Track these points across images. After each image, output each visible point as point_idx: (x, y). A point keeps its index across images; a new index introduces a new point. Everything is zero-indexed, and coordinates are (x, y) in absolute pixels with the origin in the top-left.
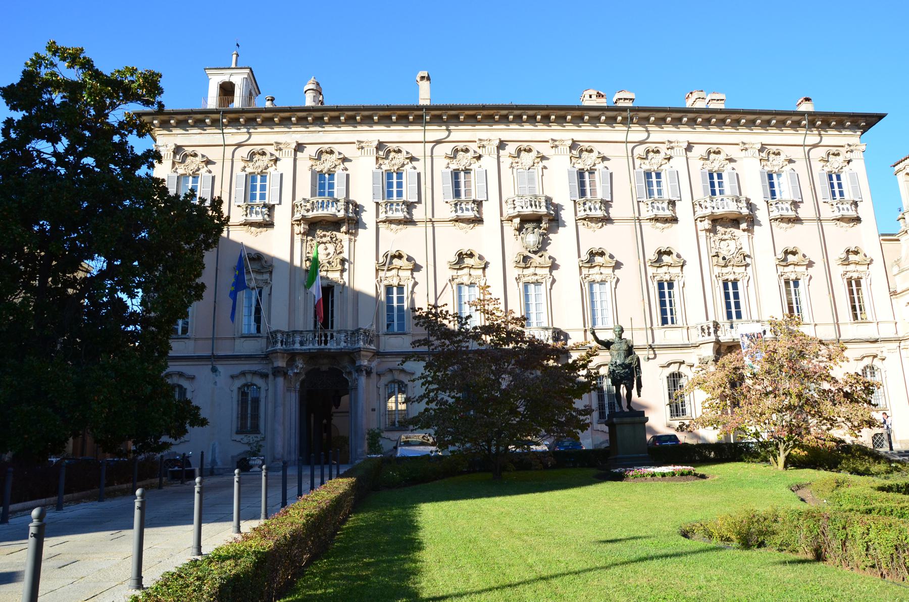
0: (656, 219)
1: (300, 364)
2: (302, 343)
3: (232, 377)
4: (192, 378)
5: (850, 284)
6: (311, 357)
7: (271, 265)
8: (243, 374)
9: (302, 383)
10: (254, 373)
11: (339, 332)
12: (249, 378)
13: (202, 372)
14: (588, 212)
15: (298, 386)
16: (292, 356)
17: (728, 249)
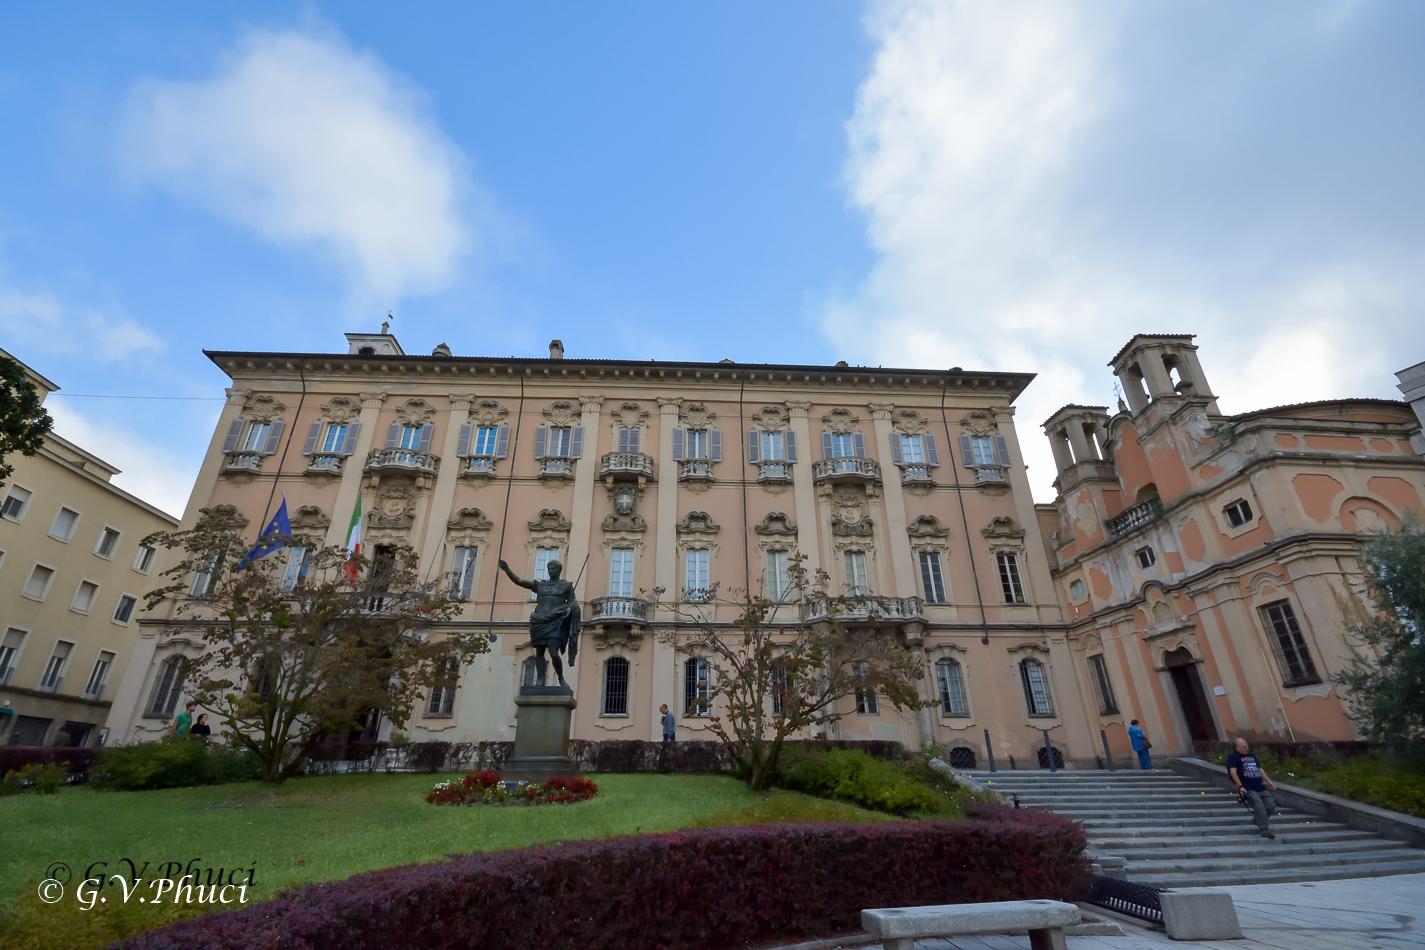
0: (766, 483)
5: (1000, 560)
7: (329, 521)
14: (692, 473)
17: (854, 516)
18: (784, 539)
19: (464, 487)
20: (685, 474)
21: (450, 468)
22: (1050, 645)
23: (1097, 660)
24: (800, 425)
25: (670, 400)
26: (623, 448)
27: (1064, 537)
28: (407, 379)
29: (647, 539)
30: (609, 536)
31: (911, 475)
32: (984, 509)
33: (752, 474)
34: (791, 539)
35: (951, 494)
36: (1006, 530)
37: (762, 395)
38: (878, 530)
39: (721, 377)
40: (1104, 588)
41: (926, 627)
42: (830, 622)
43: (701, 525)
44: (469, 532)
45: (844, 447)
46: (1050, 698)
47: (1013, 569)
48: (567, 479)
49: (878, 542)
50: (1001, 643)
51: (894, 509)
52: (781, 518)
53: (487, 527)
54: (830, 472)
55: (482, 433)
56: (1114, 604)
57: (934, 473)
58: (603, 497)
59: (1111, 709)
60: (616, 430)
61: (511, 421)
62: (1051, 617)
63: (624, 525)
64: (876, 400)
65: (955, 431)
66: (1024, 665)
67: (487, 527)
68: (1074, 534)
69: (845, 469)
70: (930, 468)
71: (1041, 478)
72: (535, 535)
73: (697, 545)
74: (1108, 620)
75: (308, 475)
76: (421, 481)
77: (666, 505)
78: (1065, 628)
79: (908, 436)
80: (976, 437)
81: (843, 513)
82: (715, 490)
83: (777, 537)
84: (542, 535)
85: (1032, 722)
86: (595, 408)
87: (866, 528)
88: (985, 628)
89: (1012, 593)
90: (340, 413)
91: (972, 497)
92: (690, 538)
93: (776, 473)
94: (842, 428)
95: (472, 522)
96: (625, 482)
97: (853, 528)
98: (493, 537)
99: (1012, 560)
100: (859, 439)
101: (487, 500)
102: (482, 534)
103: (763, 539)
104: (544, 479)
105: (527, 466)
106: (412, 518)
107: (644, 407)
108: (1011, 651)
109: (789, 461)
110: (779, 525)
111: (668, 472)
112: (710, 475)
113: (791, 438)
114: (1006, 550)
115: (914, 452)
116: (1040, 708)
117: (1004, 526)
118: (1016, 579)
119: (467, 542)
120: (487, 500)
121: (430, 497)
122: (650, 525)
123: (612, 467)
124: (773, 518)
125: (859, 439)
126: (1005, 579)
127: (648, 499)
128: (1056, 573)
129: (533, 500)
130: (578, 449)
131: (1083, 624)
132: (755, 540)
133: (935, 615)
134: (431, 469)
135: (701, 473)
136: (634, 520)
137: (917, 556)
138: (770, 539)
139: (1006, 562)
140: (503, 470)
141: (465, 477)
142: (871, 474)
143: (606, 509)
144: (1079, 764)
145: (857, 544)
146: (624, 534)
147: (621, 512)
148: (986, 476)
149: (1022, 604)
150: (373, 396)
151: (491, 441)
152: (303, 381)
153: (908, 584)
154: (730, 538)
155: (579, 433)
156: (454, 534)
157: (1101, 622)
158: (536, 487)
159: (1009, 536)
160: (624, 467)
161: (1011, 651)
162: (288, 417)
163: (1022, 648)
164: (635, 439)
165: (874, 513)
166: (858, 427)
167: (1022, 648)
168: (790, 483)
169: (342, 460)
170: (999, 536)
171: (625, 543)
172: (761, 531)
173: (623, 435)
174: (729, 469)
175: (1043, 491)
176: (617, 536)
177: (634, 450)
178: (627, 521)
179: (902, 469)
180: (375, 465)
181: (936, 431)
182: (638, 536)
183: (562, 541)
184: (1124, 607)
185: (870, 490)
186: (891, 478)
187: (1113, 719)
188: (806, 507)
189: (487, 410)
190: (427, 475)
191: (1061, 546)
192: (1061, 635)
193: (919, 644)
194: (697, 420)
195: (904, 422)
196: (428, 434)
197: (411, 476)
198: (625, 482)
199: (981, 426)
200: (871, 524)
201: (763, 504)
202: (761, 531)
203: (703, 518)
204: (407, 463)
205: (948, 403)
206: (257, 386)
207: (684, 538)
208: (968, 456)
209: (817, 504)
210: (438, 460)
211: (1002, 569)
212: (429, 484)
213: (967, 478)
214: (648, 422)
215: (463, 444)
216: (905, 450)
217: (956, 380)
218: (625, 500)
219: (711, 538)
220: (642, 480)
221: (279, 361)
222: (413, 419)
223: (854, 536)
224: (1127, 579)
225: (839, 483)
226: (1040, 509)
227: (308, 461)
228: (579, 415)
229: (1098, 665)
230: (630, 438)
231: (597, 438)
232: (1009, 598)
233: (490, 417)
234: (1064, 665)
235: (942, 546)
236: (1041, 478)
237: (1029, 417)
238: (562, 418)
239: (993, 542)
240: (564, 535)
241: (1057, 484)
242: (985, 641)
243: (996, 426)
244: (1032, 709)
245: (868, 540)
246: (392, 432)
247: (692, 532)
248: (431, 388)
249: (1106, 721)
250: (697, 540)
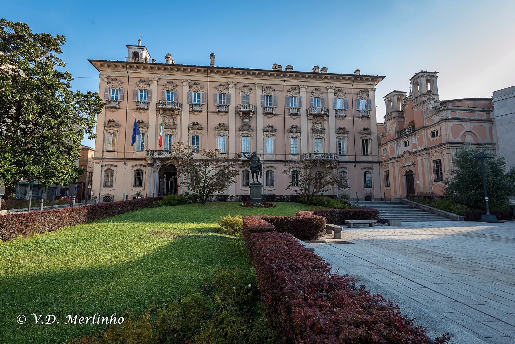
1: (158, 163)
2: (158, 155)
3: (132, 166)
4: (116, 166)
5: (363, 141)
6: (163, 160)
8: (136, 165)
9: (160, 169)
10: (141, 165)
12: (138, 168)
13: (120, 164)
15: (158, 170)
16: (155, 160)
17: (319, 127)
18: (296, 134)
19: (192, 115)
21: (186, 108)
22: (374, 167)
23: (387, 172)
24: (303, 94)
25: (259, 84)
26: (244, 102)
27: (384, 134)
28: (165, 72)
29: (254, 133)
30: (241, 132)
31: (339, 113)
32: (361, 124)
33: (286, 113)
34: (299, 134)
35: (351, 119)
36: (366, 132)
37: (291, 82)
38: (326, 131)
39: (277, 75)
40: (393, 152)
41: (338, 162)
42: (310, 160)
43: (271, 129)
44: (196, 130)
45: (318, 103)
46: (371, 182)
47: (367, 144)
48: (227, 113)
49: (326, 135)
50: (359, 167)
51: (332, 124)
52: (296, 127)
53: (202, 129)
54: (313, 112)
55: (195, 94)
56: (395, 156)
57: (346, 112)
58: (239, 119)
59: (388, 185)
60: (241, 95)
61: (205, 90)
62: (375, 159)
63: (246, 128)
64: (329, 85)
65: (355, 97)
66: (365, 173)
67: (202, 129)
68: (387, 134)
69: (317, 111)
70: (345, 111)
71: (380, 115)
72: (217, 132)
73: (269, 136)
74: (392, 161)
75: (137, 109)
76: (177, 112)
77: (259, 122)
78: (379, 162)
79: (339, 98)
80: (362, 99)
81: (316, 125)
82: (275, 118)
83: (294, 133)
84: (220, 132)
85: (365, 189)
86: (234, 86)
88: (356, 162)
89: (365, 152)
90: (143, 85)
91: (358, 121)
92: (267, 133)
93: (295, 112)
94: (317, 95)
95: (196, 127)
96: (246, 114)
98: (204, 132)
99: (367, 141)
100: (323, 99)
101: (200, 119)
102: (200, 131)
103: (290, 134)
104: (219, 112)
105: (212, 108)
106: (176, 125)
107: (251, 86)
108: (362, 169)
110: (296, 130)
111: (260, 111)
113: (300, 99)
114: (365, 138)
115: (340, 104)
116: (368, 185)
117: (367, 131)
118: (367, 147)
120: (200, 119)
121: (181, 118)
122: (254, 129)
123: (242, 109)
124: (293, 127)
125: (323, 99)
126: (363, 147)
127: (253, 119)
128: (379, 145)
129: (216, 120)
130: (229, 102)
131: (384, 161)
132: (287, 134)
133: (341, 158)
135: (270, 111)
137: (338, 140)
138: (292, 134)
139: (365, 143)
140: (204, 108)
141: (192, 111)
142: (326, 113)
143: (239, 124)
144: (377, 200)
146: (246, 132)
147: (244, 124)
148: (363, 114)
149: (367, 155)
150: (154, 79)
151: (198, 98)
153: (334, 150)
154: (280, 134)
155: (229, 96)
157: (390, 161)
158: (216, 115)
159: (367, 134)
161: (362, 169)
162: (125, 86)
163: (365, 168)
164: (248, 98)
165: (326, 126)
166: (323, 95)
167: (365, 168)
168: (299, 115)
169: (148, 103)
170: (364, 134)
171: (247, 135)
172: (289, 131)
173: (244, 96)
174: (280, 109)
175: (380, 119)
176: (244, 132)
177: (248, 103)
178: (246, 127)
179: (336, 111)
180: (160, 106)
181: (349, 97)
182: (251, 133)
183: (226, 134)
184: (397, 157)
185: (325, 117)
186: (332, 113)
187: (389, 188)
188: (304, 124)
189: (196, 86)
190: (178, 110)
191: (382, 137)
192: (378, 164)
193: (335, 167)
194: (269, 92)
195: (339, 93)
196: (177, 94)
197: (173, 110)
198: (246, 114)
199: (364, 95)
200: (324, 129)
202: (289, 131)
203: (272, 127)
204: (171, 106)
205: (354, 86)
206: (110, 74)
207: (265, 133)
208: (358, 106)
209: (308, 122)
210: (182, 105)
211: (363, 144)
212: (180, 113)
213: (356, 114)
214: (253, 92)
215: (189, 99)
216: (337, 104)
217: (357, 77)
218: (246, 120)
219: (274, 133)
220: (251, 114)
221: (117, 64)
222: (170, 88)
223: (318, 133)
224: (401, 149)
225: (315, 116)
226: (378, 125)
227: (135, 104)
228: (229, 89)
229: (387, 173)
230: (246, 98)
231: (235, 99)
232: (364, 153)
233: (197, 88)
234: (377, 173)
235: (346, 137)
236: (380, 115)
237: (380, 92)
238: (223, 90)
239: (361, 136)
240: (227, 132)
241: (385, 117)
242: (355, 166)
244: (366, 186)
245: (323, 135)
246: (163, 93)
247: (268, 131)
248: (174, 76)
249: (386, 188)
250: (269, 134)
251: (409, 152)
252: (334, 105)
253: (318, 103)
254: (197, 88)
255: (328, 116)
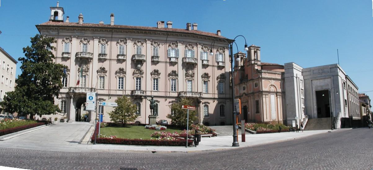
11: (87, 88)
20: (153, 60)
22: (227, 102)
26: (138, 52)
31: (205, 62)
51: (200, 71)
53: (106, 72)
87: (192, 76)
94: (190, 48)
97: (190, 75)
109: (177, 57)
110: (174, 73)
111: (149, 60)
112: (159, 60)
119: (102, 75)
120: (106, 65)
123: (136, 58)
134: (91, 57)
136: (141, 71)
145: (190, 78)
152: (58, 32)
156: (99, 73)
160: (139, 58)
172: (169, 75)
173: (138, 48)
179: (203, 61)
200: (194, 74)
201: (170, 69)
213: (216, 64)
218: (139, 66)
220: (143, 61)
223: (190, 77)
233: (104, 43)
243: (225, 52)
251: (245, 93)
252: (201, 57)
253: (189, 55)
254: (104, 43)
255: (196, 64)
